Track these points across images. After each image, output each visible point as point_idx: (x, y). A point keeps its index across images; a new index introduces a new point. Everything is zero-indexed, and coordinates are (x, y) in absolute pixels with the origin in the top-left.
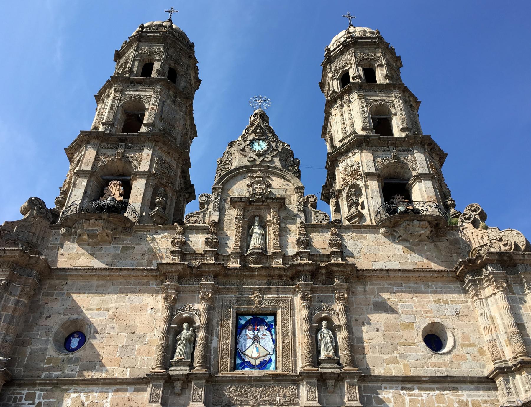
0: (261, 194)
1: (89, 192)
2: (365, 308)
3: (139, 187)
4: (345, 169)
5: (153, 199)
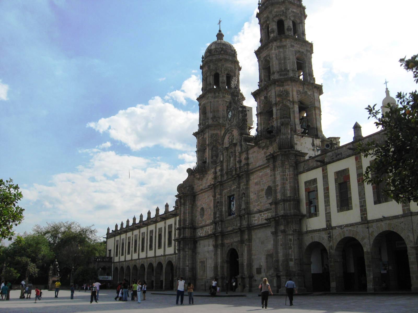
5: (212, 155)
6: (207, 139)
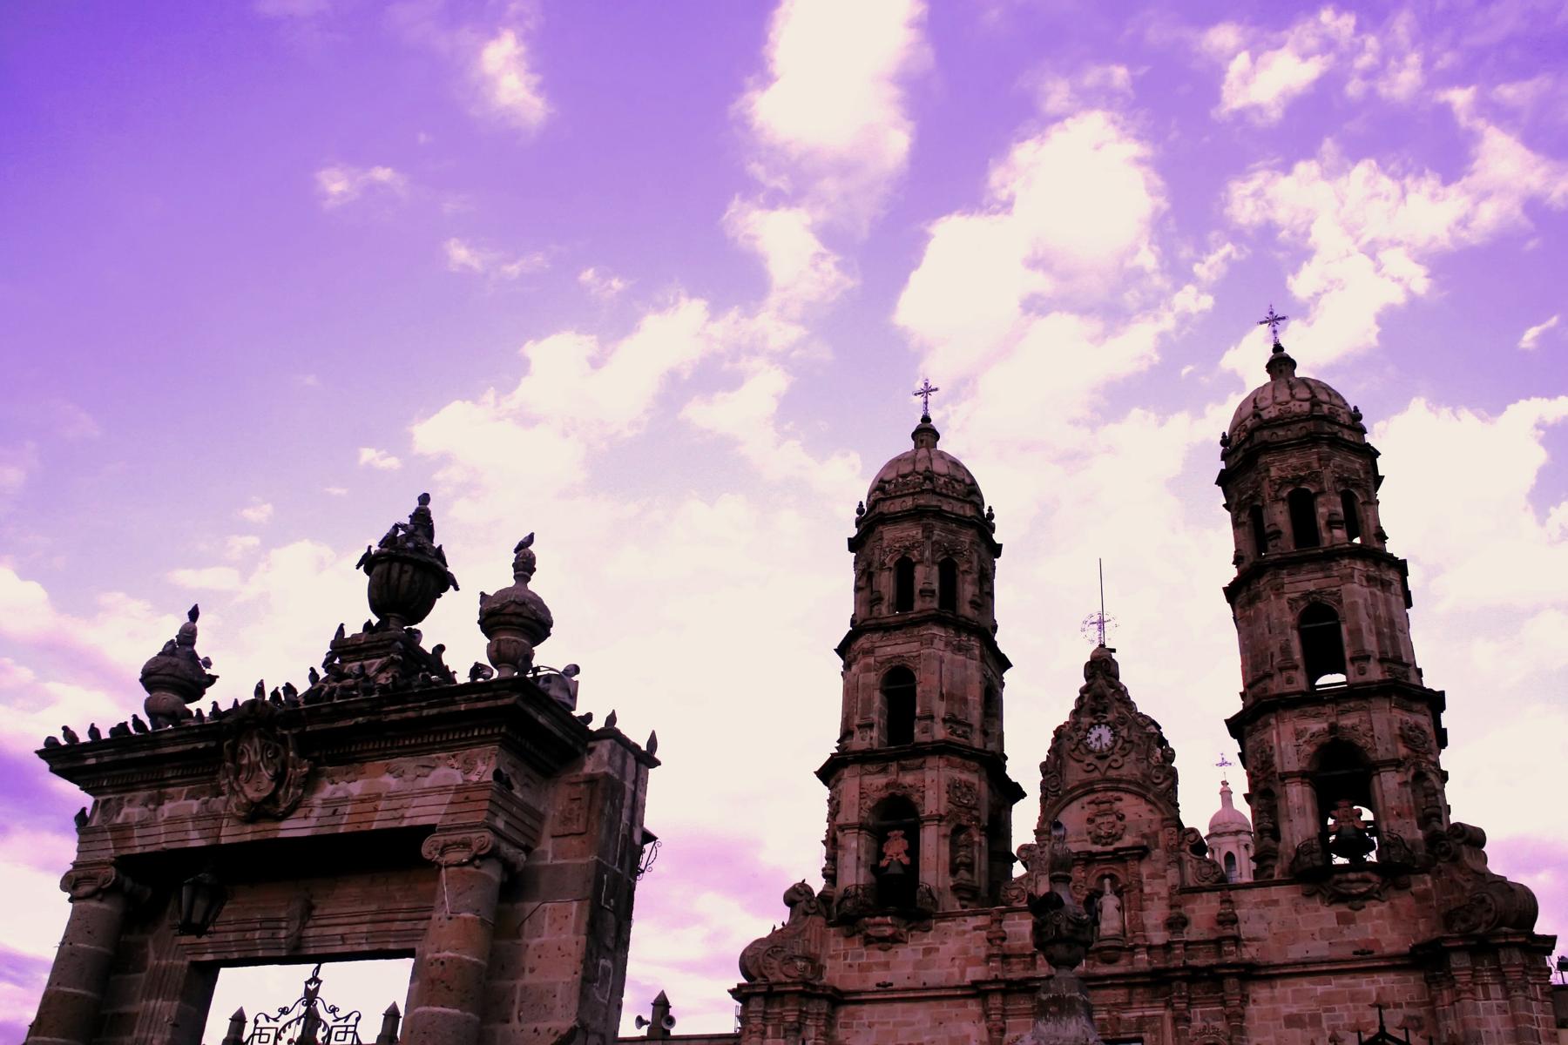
0: (1109, 835)
1: (863, 857)
2: (1271, 1024)
3: (932, 840)
4: (1254, 752)
5: (952, 859)
6: (930, 795)
